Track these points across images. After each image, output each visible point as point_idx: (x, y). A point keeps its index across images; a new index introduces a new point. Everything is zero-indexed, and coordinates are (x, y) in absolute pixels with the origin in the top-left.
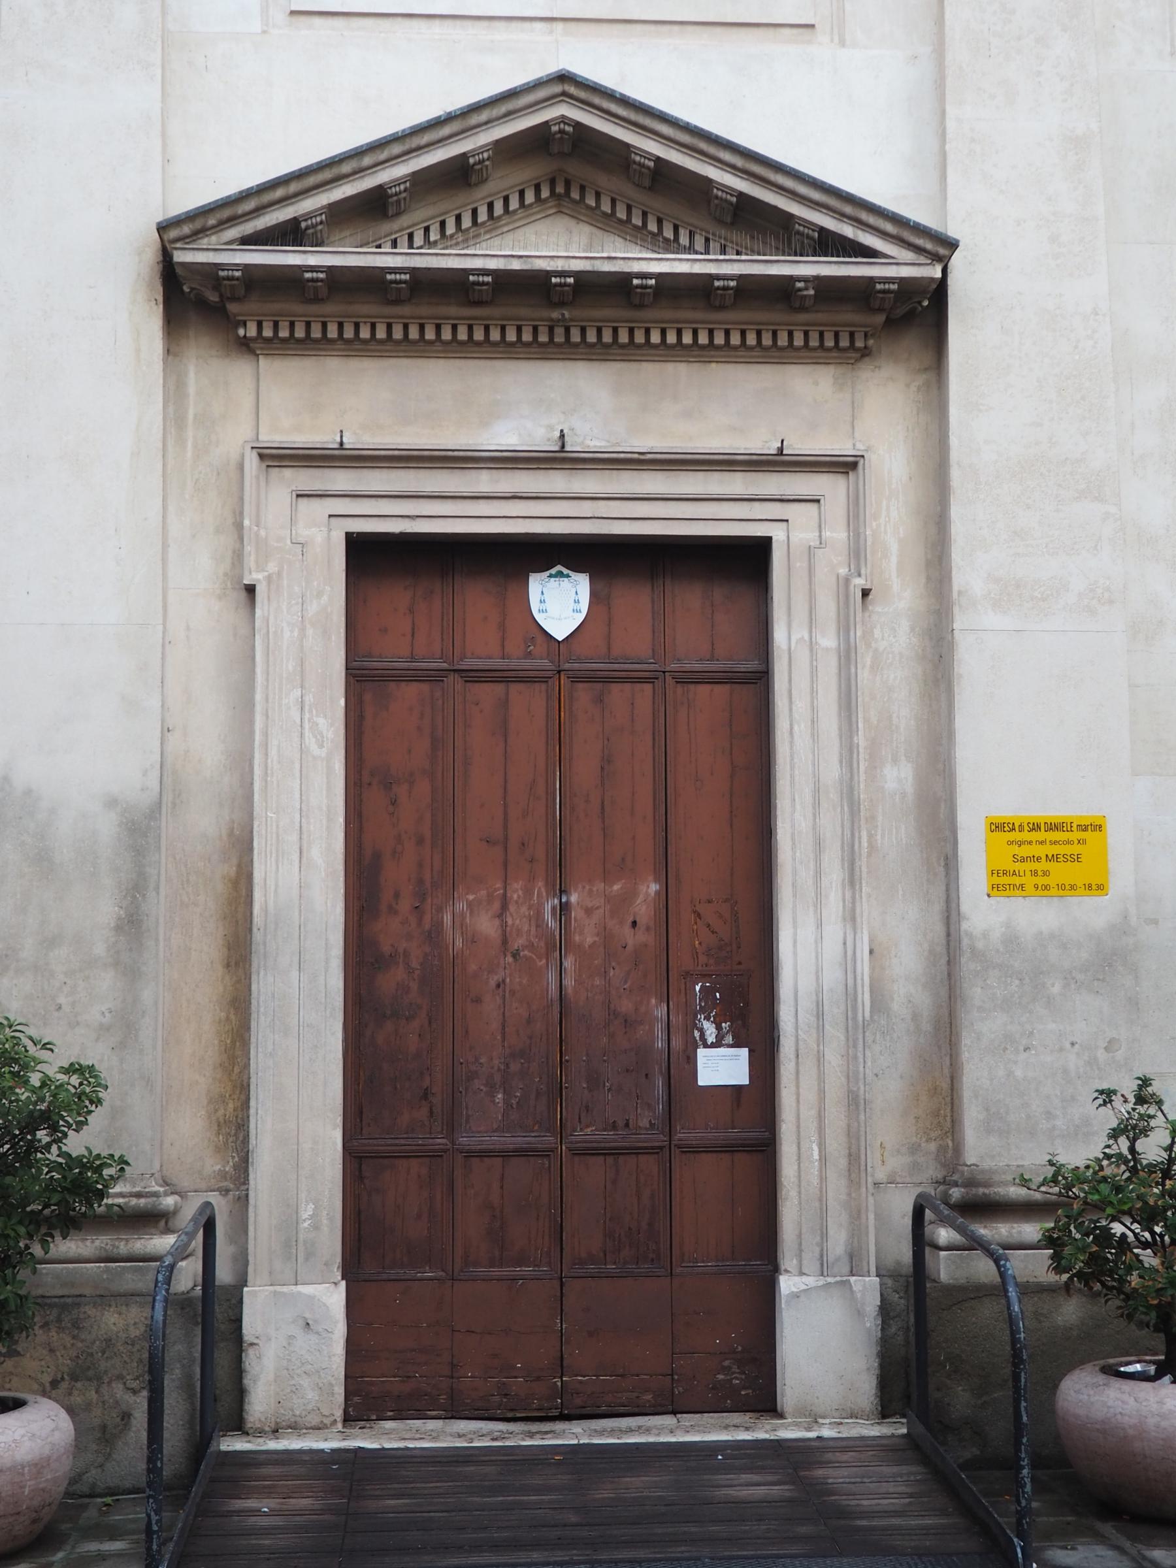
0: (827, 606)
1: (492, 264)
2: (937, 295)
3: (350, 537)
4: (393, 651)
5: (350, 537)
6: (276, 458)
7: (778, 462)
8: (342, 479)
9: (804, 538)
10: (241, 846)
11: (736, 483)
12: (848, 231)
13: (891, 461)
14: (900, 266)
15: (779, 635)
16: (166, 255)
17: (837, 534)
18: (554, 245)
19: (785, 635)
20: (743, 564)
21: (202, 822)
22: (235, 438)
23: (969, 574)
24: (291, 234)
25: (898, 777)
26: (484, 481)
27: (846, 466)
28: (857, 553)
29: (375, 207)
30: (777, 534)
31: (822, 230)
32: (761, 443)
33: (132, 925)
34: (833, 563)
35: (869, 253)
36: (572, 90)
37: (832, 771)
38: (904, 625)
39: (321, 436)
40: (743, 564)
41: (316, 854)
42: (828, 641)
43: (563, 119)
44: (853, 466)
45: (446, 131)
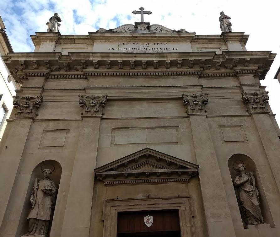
0: (188, 220)
1: (138, 172)
2: (197, 173)
7: (179, 197)
9: (183, 209)
11: (173, 201)
12: (184, 165)
13: (195, 197)
14: (192, 170)
15: (181, 224)
17: (188, 208)
18: (146, 169)
20: (175, 213)
23: (208, 213)
24: (112, 170)
27: (188, 198)
28: (191, 211)
29: (123, 165)
30: (179, 209)
31: (181, 165)
32: (176, 195)
35: (188, 168)
36: (148, 150)
38: (199, 222)
40: (175, 213)
42: (188, 225)
43: (147, 154)
44: (189, 198)
45: (133, 156)
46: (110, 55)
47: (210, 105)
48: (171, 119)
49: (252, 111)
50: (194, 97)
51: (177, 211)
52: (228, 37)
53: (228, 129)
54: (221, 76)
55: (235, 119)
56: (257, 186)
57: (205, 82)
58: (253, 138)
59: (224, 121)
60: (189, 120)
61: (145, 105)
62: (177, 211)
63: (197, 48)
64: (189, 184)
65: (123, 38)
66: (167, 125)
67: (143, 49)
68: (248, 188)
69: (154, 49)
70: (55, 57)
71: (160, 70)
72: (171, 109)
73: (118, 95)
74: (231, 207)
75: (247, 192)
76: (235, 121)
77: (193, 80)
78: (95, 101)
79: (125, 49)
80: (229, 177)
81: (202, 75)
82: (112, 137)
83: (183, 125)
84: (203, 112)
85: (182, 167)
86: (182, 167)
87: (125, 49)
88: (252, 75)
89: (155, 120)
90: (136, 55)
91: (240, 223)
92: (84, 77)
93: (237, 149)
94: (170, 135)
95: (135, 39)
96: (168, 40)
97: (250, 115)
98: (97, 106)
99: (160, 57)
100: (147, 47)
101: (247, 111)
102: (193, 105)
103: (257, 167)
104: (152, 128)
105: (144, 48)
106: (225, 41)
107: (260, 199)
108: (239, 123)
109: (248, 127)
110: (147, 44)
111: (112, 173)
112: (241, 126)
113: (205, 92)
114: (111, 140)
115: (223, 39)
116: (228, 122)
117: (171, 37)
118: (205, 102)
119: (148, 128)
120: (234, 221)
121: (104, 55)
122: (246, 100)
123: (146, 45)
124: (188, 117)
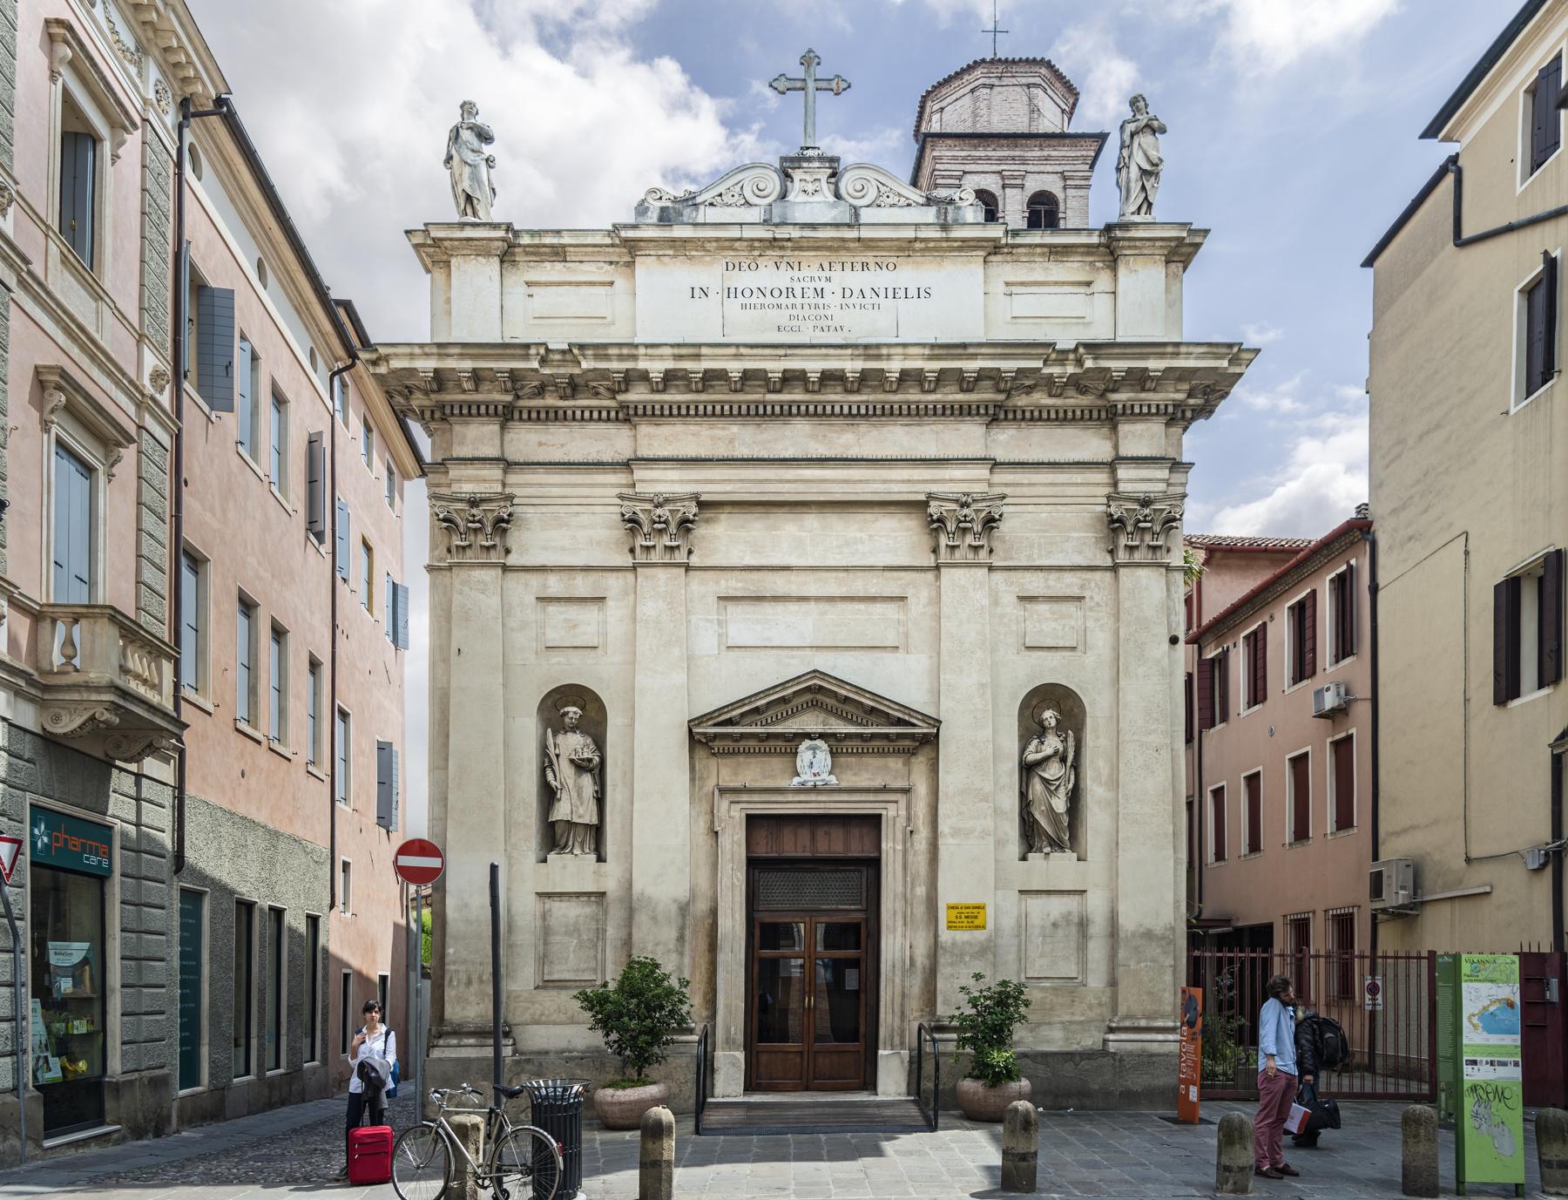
0: (899, 836)
3: (748, 816)
4: (762, 851)
5: (748, 816)
6: (723, 791)
7: (885, 790)
8: (745, 797)
9: (893, 813)
10: (714, 912)
11: (871, 797)
13: (922, 789)
14: (924, 729)
15: (884, 846)
16: (690, 731)
17: (903, 813)
19: (886, 845)
20: (874, 821)
21: (702, 906)
22: (711, 783)
24: (729, 722)
25: (921, 891)
26: (790, 798)
28: (909, 819)
30: (884, 812)
32: (878, 783)
33: (681, 938)
34: (901, 822)
35: (914, 725)
37: (900, 889)
39: (737, 784)
40: (874, 821)
41: (737, 916)
42: (899, 847)
46: (704, 351)
47: (1004, 527)
48: (887, 574)
49: (1122, 556)
50: (964, 505)
51: (879, 816)
52: (1126, 243)
53: (1043, 608)
54: (1063, 418)
55: (1069, 578)
56: (1076, 767)
57: (1008, 442)
58: (1101, 640)
59: (1035, 583)
60: (938, 578)
61: (812, 520)
62: (879, 816)
63: (1007, 284)
64: (913, 759)
65: (737, 244)
66: (873, 592)
67: (810, 293)
68: (1053, 771)
69: (848, 293)
70: (526, 357)
71: (864, 398)
72: (896, 539)
73: (729, 487)
74: (997, 812)
75: (1046, 781)
76: (1069, 583)
77: (967, 437)
78: (663, 512)
79: (747, 293)
80: (1011, 743)
81: (1002, 416)
82: (720, 623)
83: (919, 589)
84: (983, 556)
85: (900, 722)
86: (900, 722)
87: (747, 293)
88: (1163, 420)
89: (842, 575)
90: (789, 352)
91: (1014, 846)
92: (621, 415)
93: (1050, 670)
94: (877, 622)
95: (782, 248)
96: (900, 249)
97: (1114, 568)
98: (673, 528)
99: (868, 357)
100: (823, 284)
101: (1111, 552)
102: (959, 530)
103: (1089, 721)
104: (831, 599)
105: (813, 285)
106: (1112, 253)
107: (1075, 797)
108: (1076, 592)
109: (1098, 604)
110: (826, 266)
111: (729, 730)
112: (1080, 598)
113: (1002, 477)
114: (720, 635)
115: (1108, 247)
116: (1048, 587)
117: (916, 239)
118: (990, 522)
119: (818, 599)
120: (999, 844)
121: (684, 351)
122: (1113, 521)
123: (821, 273)
124: (937, 568)
